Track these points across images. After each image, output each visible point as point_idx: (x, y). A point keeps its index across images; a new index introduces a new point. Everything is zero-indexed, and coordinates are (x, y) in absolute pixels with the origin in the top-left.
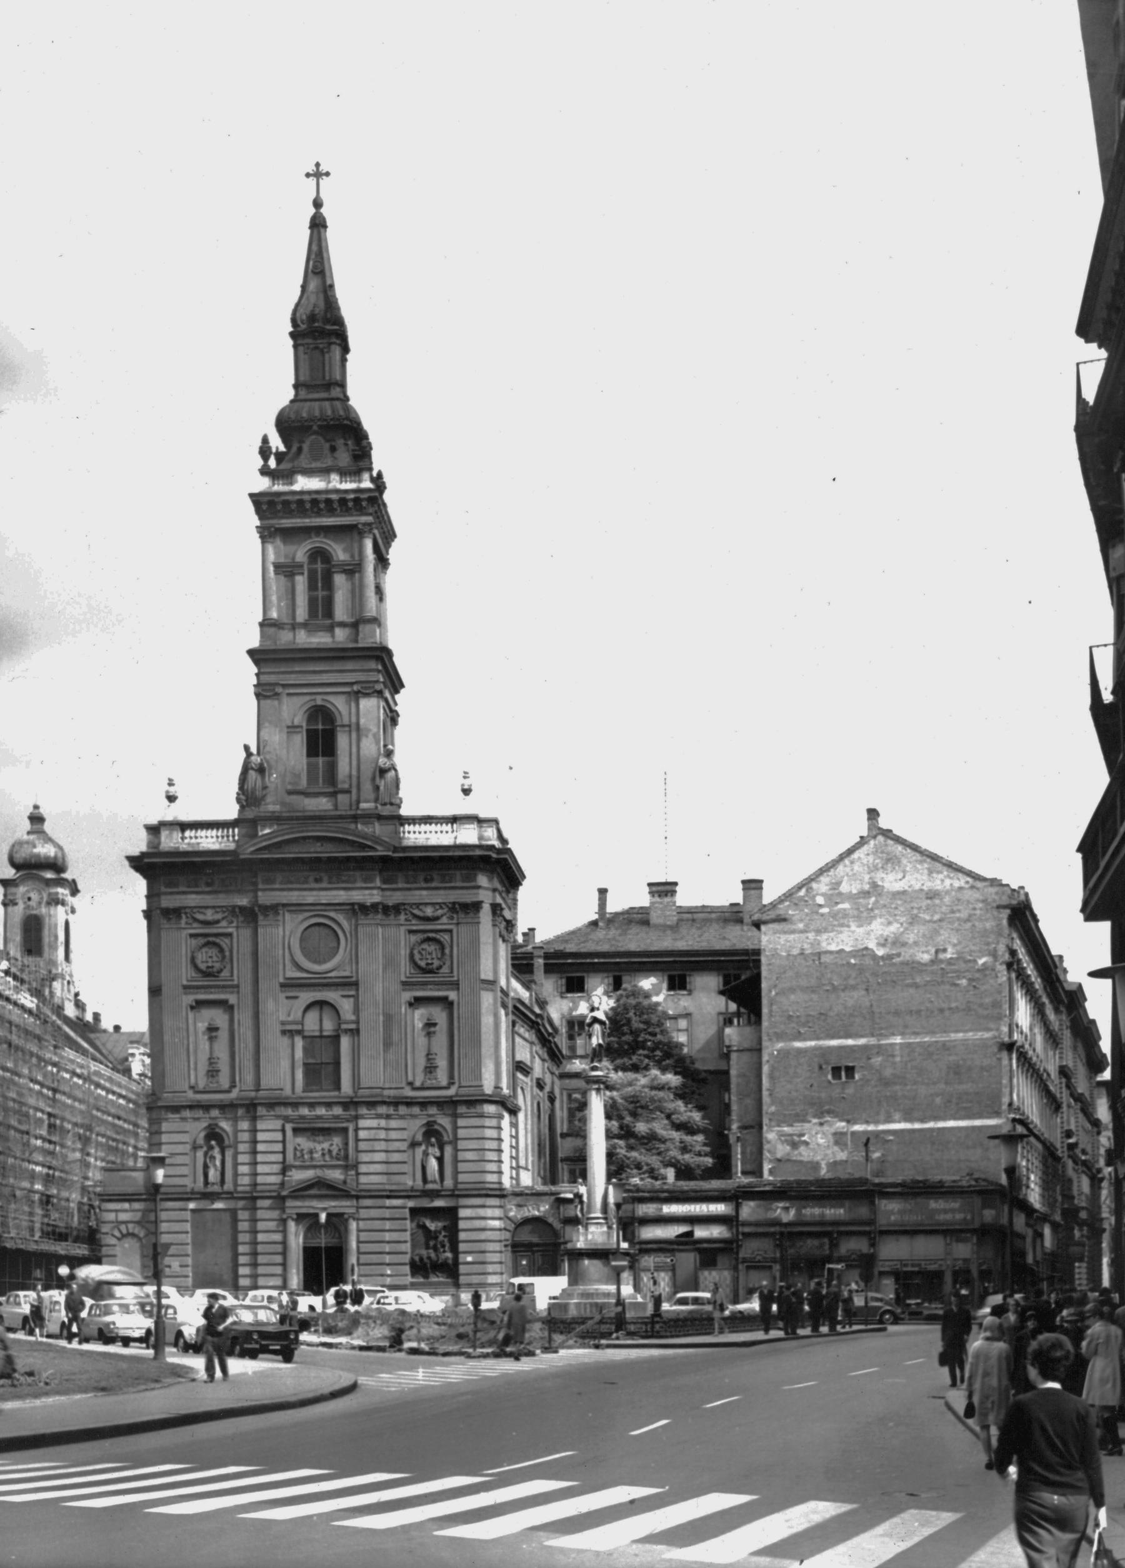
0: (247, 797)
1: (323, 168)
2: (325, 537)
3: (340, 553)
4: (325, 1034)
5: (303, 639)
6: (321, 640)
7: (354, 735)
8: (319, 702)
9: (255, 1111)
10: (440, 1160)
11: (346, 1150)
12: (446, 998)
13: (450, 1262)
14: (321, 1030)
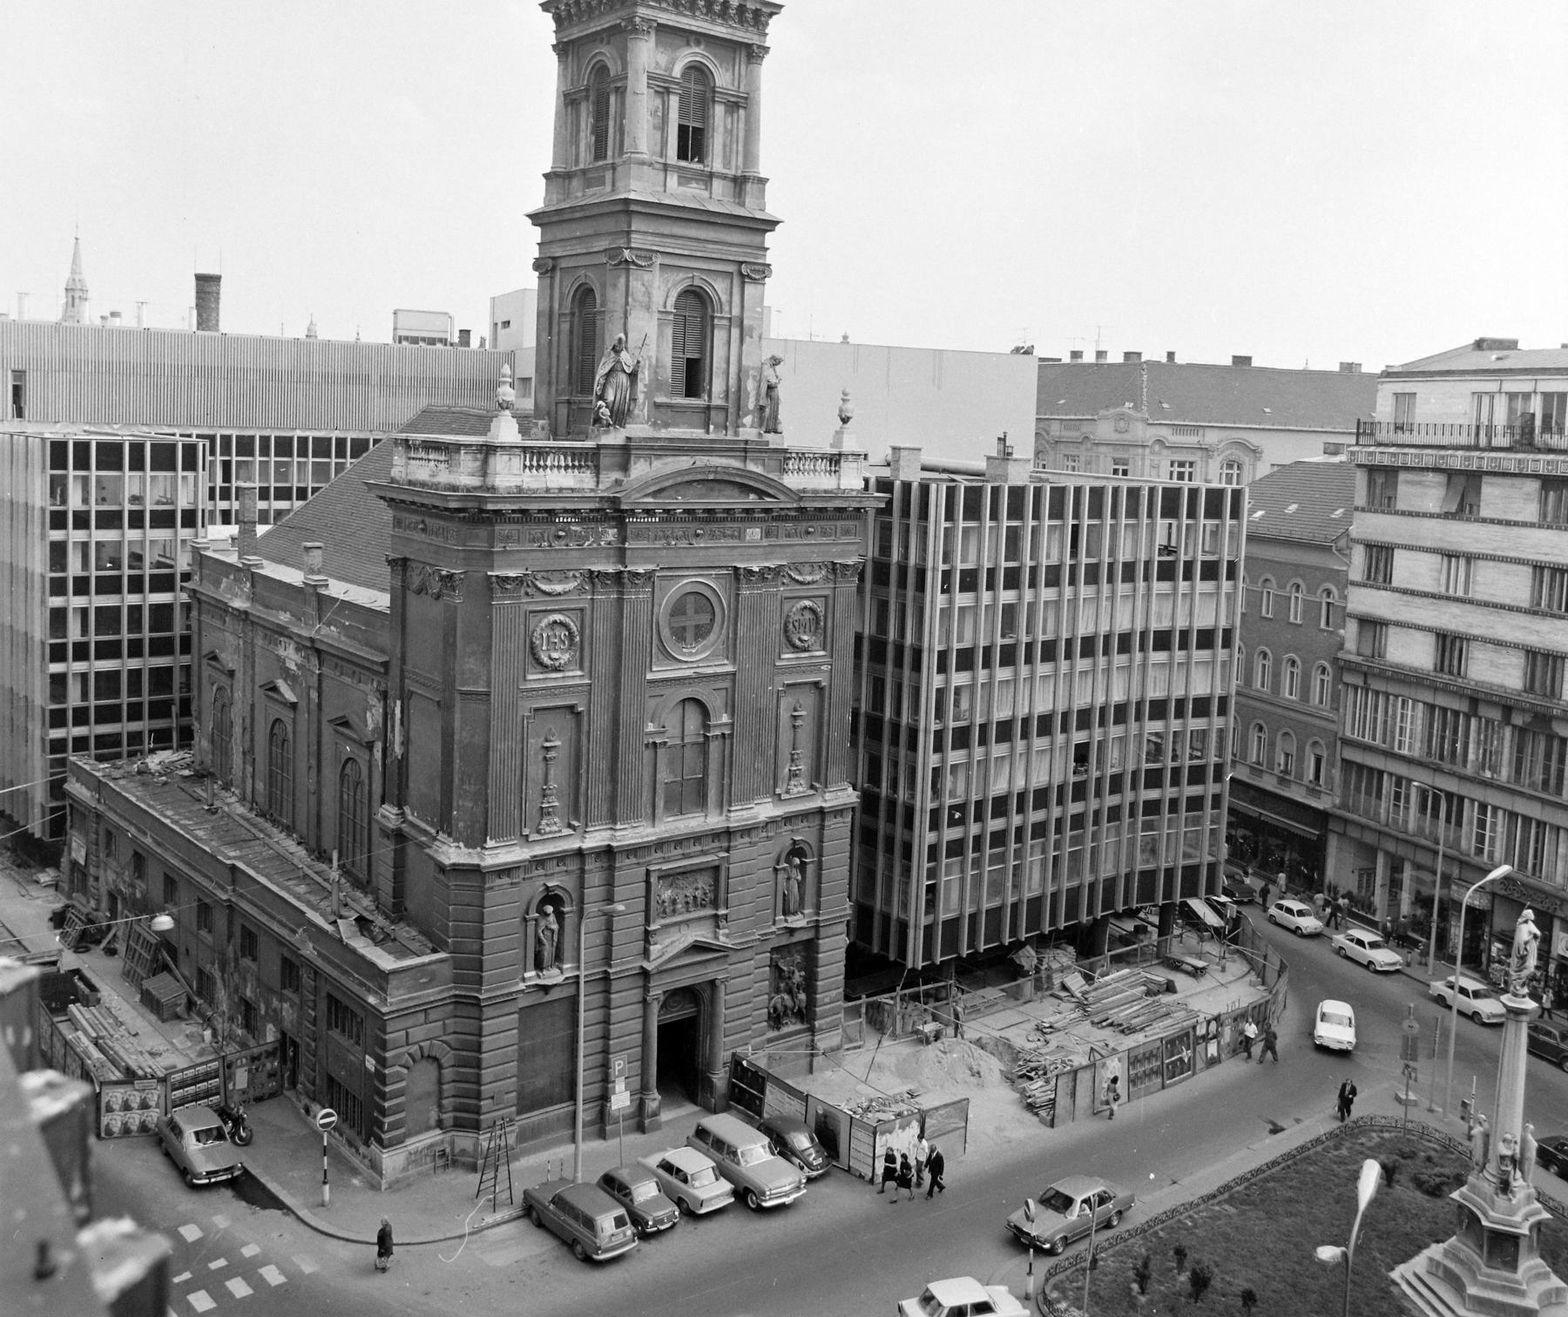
3: (722, 79)
7: (735, 332)
8: (697, 282)
10: (801, 884)
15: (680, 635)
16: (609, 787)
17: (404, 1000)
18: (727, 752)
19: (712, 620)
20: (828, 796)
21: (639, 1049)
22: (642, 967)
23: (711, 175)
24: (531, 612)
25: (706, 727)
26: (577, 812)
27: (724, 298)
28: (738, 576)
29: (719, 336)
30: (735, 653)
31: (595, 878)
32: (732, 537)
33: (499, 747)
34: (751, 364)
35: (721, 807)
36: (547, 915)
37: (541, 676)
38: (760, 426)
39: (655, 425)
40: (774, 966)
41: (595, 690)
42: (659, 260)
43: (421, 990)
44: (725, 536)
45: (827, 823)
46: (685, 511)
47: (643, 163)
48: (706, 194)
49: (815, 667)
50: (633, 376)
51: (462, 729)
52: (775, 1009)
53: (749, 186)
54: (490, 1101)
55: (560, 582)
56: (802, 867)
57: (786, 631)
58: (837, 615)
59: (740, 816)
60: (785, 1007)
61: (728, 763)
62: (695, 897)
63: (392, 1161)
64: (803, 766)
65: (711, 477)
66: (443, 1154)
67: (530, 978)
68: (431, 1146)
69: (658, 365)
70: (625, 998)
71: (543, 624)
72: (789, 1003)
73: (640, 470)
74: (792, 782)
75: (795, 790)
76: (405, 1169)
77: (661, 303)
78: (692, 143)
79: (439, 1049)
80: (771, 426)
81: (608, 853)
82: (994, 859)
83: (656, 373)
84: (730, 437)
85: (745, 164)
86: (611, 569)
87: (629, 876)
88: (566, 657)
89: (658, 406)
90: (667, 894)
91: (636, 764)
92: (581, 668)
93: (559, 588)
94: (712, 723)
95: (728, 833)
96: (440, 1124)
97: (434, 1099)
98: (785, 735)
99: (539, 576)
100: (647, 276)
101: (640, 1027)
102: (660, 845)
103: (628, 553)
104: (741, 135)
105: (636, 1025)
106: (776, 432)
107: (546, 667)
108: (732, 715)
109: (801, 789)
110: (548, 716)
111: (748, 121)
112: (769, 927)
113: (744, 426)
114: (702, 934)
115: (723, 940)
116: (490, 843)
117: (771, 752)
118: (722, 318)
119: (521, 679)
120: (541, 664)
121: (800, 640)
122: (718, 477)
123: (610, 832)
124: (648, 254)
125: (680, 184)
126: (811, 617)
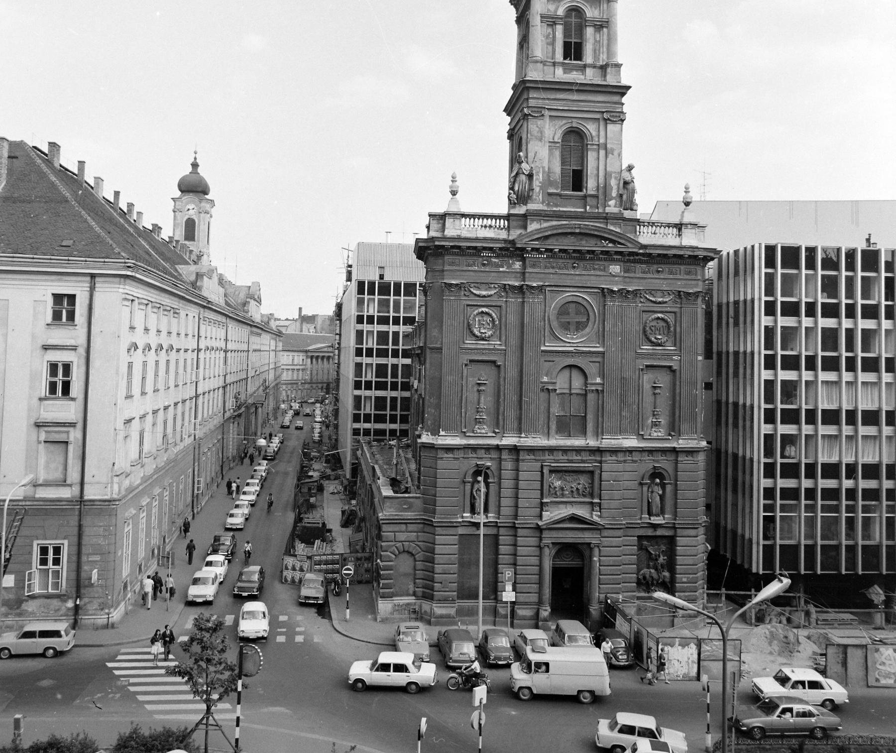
0: (519, 197)
5: (560, 75)
6: (575, 77)
7: (602, 152)
8: (574, 125)
9: (518, 455)
10: (662, 497)
11: (592, 487)
12: (670, 367)
13: (667, 580)
15: (566, 327)
16: (518, 412)
17: (392, 515)
18: (600, 402)
19: (588, 319)
20: (681, 441)
21: (537, 576)
22: (537, 524)
23: (585, 66)
24: (468, 305)
25: (586, 384)
26: (498, 426)
27: (594, 133)
28: (605, 293)
29: (591, 156)
30: (604, 341)
31: (508, 465)
32: (600, 270)
33: (448, 379)
34: (613, 170)
35: (597, 436)
36: (479, 482)
37: (474, 342)
38: (621, 206)
39: (548, 205)
40: (641, 548)
41: (509, 353)
42: (547, 113)
43: (401, 512)
44: (594, 269)
45: (679, 459)
46: (560, 250)
47: (537, 62)
48: (582, 77)
49: (669, 356)
50: (530, 176)
51: (430, 368)
52: (645, 578)
53: (609, 70)
54: (440, 584)
55: (486, 290)
56: (663, 486)
57: (644, 331)
58: (684, 325)
59: (608, 442)
60: (652, 577)
61: (600, 410)
62: (577, 489)
63: (384, 606)
64: (663, 420)
65: (577, 231)
66: (415, 612)
67: (467, 517)
68: (408, 604)
69: (549, 173)
70: (527, 542)
71: (475, 313)
72: (655, 576)
73: (533, 226)
74: (653, 429)
75: (655, 434)
76: (392, 613)
77: (551, 137)
78: (573, 50)
79: (413, 548)
80: (628, 206)
81: (515, 450)
82: (825, 509)
83: (549, 177)
84: (601, 210)
85: (608, 58)
86: (517, 284)
87: (529, 469)
88: (490, 333)
89: (550, 194)
90: (558, 483)
91: (534, 401)
92: (500, 340)
93: (484, 293)
94: (590, 381)
95: (599, 451)
96: (414, 594)
97: (412, 577)
98: (648, 398)
99: (472, 285)
100: (539, 122)
101: (537, 563)
102: (551, 450)
103: (527, 275)
104: (605, 42)
105: (535, 560)
106: (632, 210)
107: (477, 337)
108: (603, 379)
109: (660, 434)
110: (481, 366)
111: (609, 34)
112: (636, 520)
113: (609, 206)
114: (582, 512)
115: (596, 518)
116: (442, 433)
117: (635, 407)
118: (593, 144)
119: (461, 342)
120: (474, 335)
121: (656, 338)
122: (583, 231)
123: (518, 439)
124: (539, 110)
125: (565, 73)
126: (664, 325)
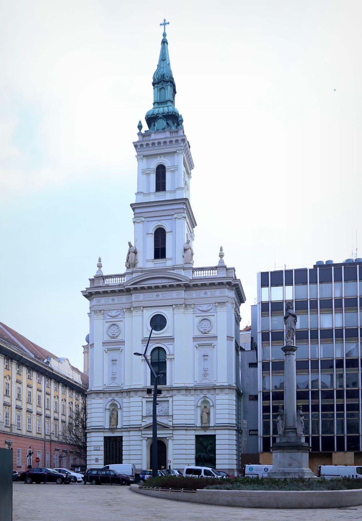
1: (167, 22)
2: (164, 158)
4: (160, 361)
14: (159, 359)
